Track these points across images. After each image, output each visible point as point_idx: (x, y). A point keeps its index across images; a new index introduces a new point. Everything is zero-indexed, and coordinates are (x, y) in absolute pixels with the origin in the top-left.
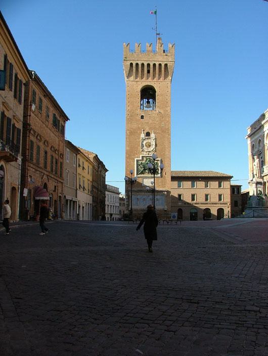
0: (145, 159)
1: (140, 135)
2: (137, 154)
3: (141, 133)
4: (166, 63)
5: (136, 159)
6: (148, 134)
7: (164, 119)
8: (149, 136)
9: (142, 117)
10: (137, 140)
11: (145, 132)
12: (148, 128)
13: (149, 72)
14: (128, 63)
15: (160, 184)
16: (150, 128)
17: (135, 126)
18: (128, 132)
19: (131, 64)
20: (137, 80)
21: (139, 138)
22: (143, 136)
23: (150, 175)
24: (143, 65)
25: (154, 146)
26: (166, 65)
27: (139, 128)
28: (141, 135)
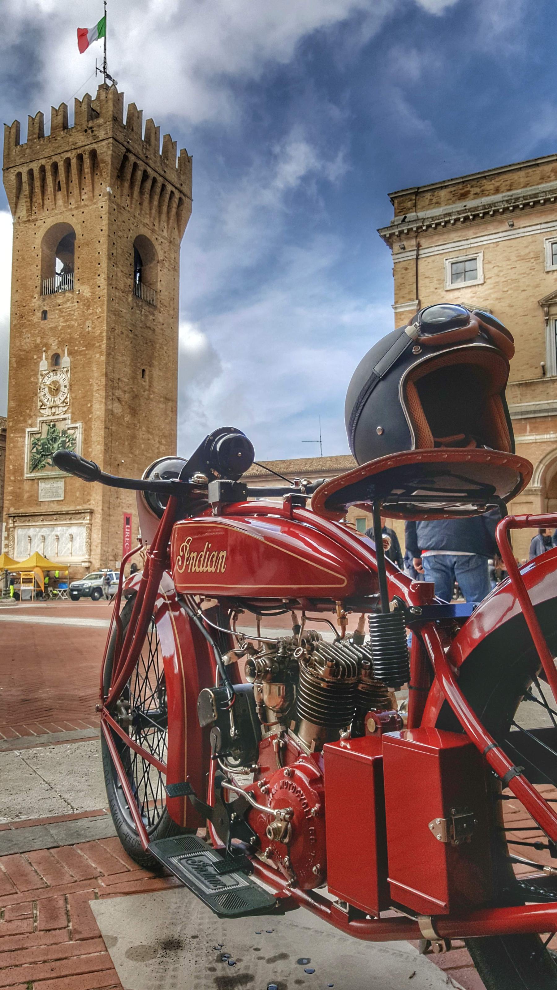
0: (45, 428)
1: (37, 364)
2: (30, 417)
3: (41, 358)
5: (28, 430)
6: (56, 359)
10: (32, 379)
11: (50, 353)
16: (61, 344)
17: (28, 341)
18: (14, 360)
21: (36, 375)
22: (44, 365)
24: (42, 169)
26: (93, 154)
27: (37, 346)
28: (41, 364)
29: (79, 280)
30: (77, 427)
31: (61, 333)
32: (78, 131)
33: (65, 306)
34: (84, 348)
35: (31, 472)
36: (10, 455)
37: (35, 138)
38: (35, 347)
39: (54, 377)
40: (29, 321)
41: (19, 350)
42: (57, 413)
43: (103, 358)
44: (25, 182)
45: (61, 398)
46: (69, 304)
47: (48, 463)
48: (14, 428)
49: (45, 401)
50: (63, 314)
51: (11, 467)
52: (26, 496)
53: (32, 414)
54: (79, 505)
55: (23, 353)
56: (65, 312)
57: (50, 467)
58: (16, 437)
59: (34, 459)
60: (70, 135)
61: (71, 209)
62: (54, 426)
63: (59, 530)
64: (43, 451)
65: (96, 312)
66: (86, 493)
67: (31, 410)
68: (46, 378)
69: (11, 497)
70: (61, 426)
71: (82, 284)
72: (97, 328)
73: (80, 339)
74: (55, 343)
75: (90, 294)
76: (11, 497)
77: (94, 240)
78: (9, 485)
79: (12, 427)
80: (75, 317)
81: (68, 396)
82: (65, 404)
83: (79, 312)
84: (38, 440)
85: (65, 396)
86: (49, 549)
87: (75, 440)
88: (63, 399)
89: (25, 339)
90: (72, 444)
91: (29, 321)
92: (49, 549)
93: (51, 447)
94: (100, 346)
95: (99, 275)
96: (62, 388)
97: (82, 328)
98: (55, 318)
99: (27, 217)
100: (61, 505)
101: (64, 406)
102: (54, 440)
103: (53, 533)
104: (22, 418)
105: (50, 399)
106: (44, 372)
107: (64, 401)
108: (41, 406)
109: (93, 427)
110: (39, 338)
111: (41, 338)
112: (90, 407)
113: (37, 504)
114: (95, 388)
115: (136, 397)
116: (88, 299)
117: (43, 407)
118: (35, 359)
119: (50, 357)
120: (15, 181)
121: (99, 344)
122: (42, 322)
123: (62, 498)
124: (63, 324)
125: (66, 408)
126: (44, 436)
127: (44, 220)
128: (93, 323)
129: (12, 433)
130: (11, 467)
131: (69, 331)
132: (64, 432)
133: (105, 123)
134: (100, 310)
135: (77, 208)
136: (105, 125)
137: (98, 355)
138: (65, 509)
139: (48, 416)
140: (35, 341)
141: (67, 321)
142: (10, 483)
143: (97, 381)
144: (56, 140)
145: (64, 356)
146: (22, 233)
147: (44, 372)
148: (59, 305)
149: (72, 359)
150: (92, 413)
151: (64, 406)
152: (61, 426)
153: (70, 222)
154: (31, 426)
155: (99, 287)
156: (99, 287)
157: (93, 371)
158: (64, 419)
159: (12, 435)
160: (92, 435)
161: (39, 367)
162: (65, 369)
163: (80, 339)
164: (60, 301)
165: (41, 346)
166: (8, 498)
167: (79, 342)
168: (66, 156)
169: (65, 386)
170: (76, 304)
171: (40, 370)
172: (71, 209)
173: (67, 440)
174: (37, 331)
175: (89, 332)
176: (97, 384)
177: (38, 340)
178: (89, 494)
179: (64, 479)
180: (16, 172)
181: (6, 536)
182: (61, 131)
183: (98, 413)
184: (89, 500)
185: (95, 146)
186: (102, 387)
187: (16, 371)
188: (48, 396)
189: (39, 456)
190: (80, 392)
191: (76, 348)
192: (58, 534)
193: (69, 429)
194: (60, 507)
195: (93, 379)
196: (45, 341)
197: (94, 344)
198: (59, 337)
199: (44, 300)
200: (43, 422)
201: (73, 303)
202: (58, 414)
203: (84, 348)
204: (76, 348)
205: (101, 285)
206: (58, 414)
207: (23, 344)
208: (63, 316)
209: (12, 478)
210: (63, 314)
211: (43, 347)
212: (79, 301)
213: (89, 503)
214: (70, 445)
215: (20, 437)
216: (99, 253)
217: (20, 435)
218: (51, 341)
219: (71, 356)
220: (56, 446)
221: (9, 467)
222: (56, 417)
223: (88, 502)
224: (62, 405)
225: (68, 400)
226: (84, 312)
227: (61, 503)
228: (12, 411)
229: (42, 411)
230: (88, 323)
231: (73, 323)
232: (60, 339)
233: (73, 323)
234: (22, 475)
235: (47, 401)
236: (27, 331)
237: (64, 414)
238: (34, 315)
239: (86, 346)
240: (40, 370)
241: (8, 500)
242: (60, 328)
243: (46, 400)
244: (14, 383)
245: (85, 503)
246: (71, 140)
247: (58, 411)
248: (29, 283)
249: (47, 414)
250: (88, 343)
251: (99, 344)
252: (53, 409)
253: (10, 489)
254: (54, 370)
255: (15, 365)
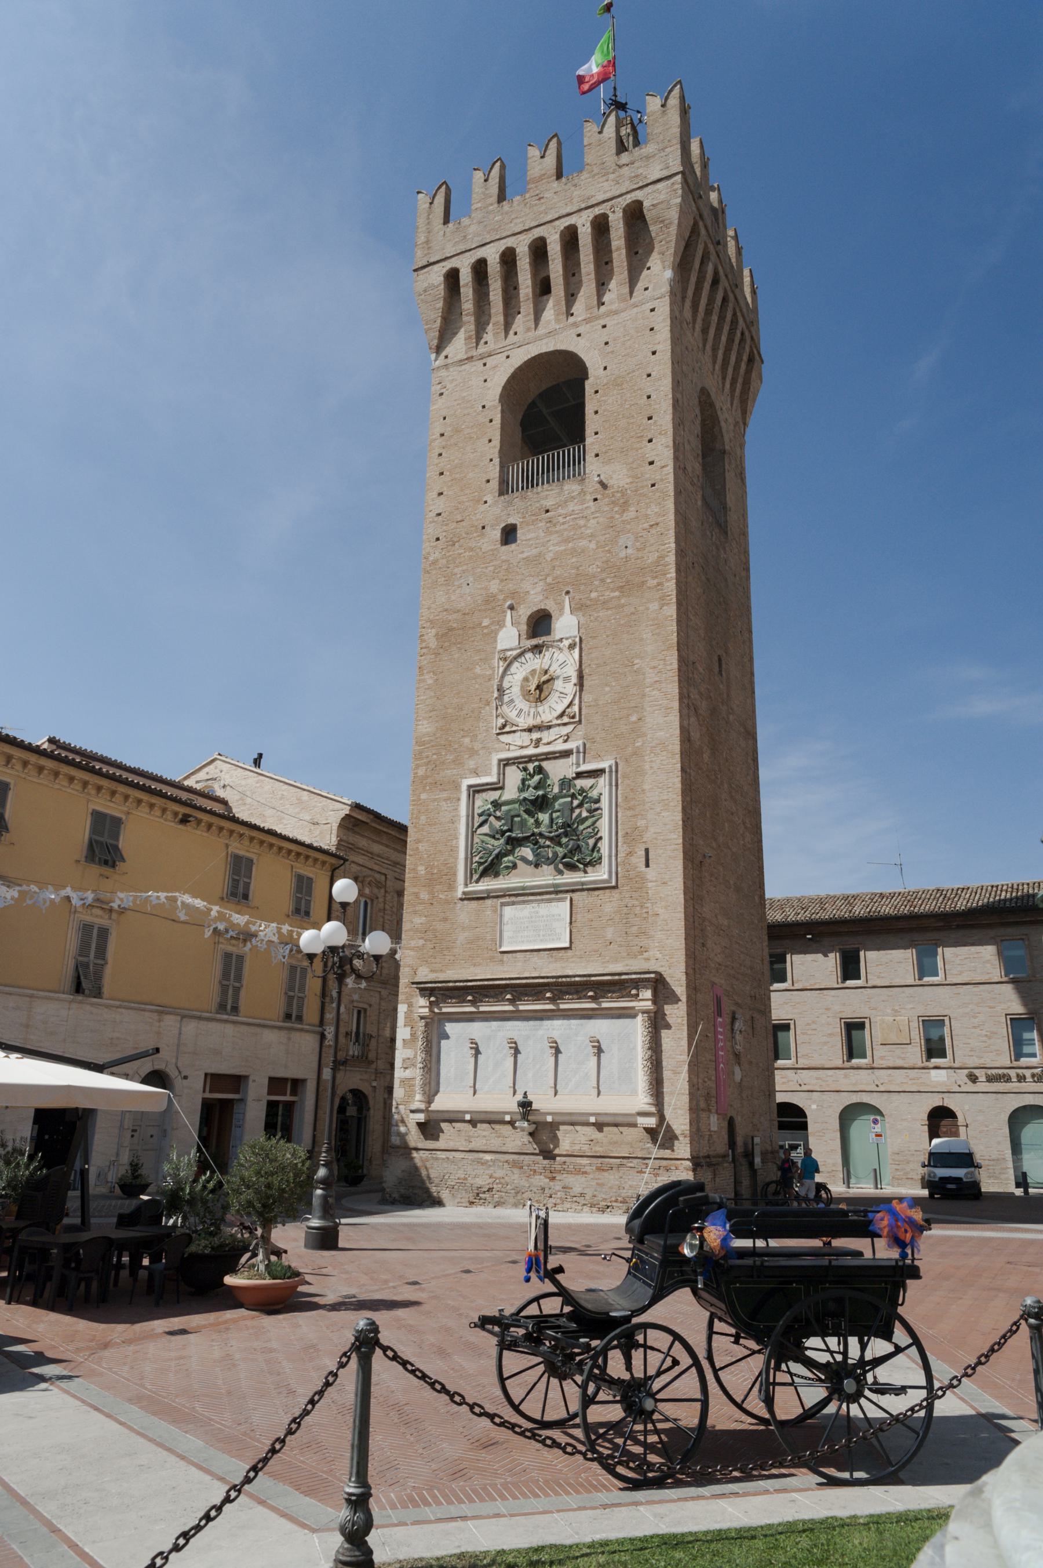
0: (514, 776)
2: (473, 752)
3: (501, 624)
4: (629, 198)
7: (631, 514)
8: (548, 632)
9: (509, 534)
10: (478, 670)
11: (525, 612)
12: (541, 585)
13: (543, 288)
14: (436, 276)
15: (610, 933)
19: (452, 277)
20: (482, 349)
23: (546, 876)
25: (570, 688)
27: (490, 600)
28: (502, 635)
29: (597, 455)
30: (602, 771)
31: (554, 567)
32: (594, 175)
33: (561, 511)
34: (617, 594)
35: (477, 882)
36: (418, 841)
37: (492, 205)
38: (487, 602)
39: (533, 662)
40: (471, 549)
41: (446, 610)
42: (544, 741)
43: (671, 611)
44: (466, 285)
45: (553, 706)
46: (571, 506)
47: (524, 859)
48: (429, 780)
49: (512, 715)
50: (558, 528)
51: (422, 870)
52: (462, 937)
53: (477, 746)
54: (616, 961)
55: (455, 616)
56: (563, 524)
57: (531, 869)
58: (435, 800)
59: (484, 849)
60: (575, 186)
61: (575, 325)
62: (540, 770)
63: (556, 1028)
64: (510, 830)
65: (647, 515)
66: (634, 929)
67: (474, 739)
68: (516, 664)
69: (421, 942)
70: (558, 770)
71: (609, 461)
72: (647, 549)
73: (604, 575)
74: (539, 589)
75: (628, 480)
76: (421, 942)
77: (637, 373)
78: (415, 912)
79: (426, 777)
80: (589, 531)
81: (577, 701)
82: (566, 720)
83: (601, 520)
84: (496, 804)
85: (567, 702)
86: (530, 1075)
87: (598, 801)
88: (560, 709)
89: (460, 587)
90: (589, 811)
91: (471, 549)
92: (530, 1075)
93: (532, 821)
94: (659, 584)
95: (650, 441)
96: (558, 685)
97: (609, 551)
98: (537, 538)
99: (466, 353)
100: (561, 959)
101: (565, 724)
102: (541, 803)
103: (541, 1032)
104: (450, 757)
105: (526, 709)
106: (509, 653)
107: (564, 712)
108: (504, 726)
109: (647, 767)
110: (497, 581)
111: (502, 581)
112: (635, 723)
113: (492, 959)
114: (651, 677)
115: (714, 711)
116: (623, 492)
117: (507, 729)
118: (486, 627)
119: (524, 619)
120: (442, 286)
121: (655, 582)
122: (505, 548)
123: (567, 945)
124: (557, 548)
125: (570, 728)
126: (511, 792)
127: (506, 354)
128: (636, 539)
129: (424, 790)
130: (422, 870)
131: (574, 560)
132: (566, 783)
133: (663, 150)
134: (656, 510)
135: (588, 321)
136: (663, 154)
137: (654, 606)
138: (576, 968)
139: (522, 747)
140: (486, 588)
141: (567, 541)
142: (420, 908)
143: (655, 663)
144: (539, 199)
145: (561, 614)
146: (455, 383)
147: (509, 653)
148: (547, 511)
149: (583, 620)
150: (644, 735)
151: (565, 724)
152: (558, 770)
153: (571, 349)
154: (476, 773)
155: (651, 463)
156: (651, 463)
157: (642, 640)
158: (566, 754)
159: (424, 796)
160: (646, 787)
161: (496, 641)
162: (566, 643)
163: (604, 575)
164: (548, 503)
165: (501, 597)
166: (413, 943)
167: (603, 580)
168: (567, 224)
169: (567, 679)
170: (592, 503)
171: (500, 646)
172: (575, 325)
173: (576, 803)
174: (493, 568)
175: (627, 558)
176: (654, 667)
177: (494, 587)
178: (643, 933)
179: (568, 896)
180: (444, 271)
181: (408, 1036)
182: (553, 181)
183: (661, 734)
184: (643, 950)
185: (638, 195)
186: (670, 674)
187: (437, 654)
188: (521, 704)
189: (496, 843)
190: (607, 689)
191: (594, 595)
192: (556, 1035)
193: (579, 775)
194: (558, 965)
195: (642, 658)
196: (511, 586)
197: (643, 583)
198: (548, 575)
199: (510, 503)
200: (506, 763)
201: (583, 502)
202: (549, 743)
203: (617, 594)
204: (594, 595)
205: (656, 459)
206: (549, 743)
207: (453, 598)
208: (557, 532)
209: (424, 895)
210: (558, 528)
211: (505, 600)
212: (599, 497)
213: (646, 955)
214: (585, 814)
215: (445, 800)
216: (649, 397)
217: (444, 795)
218: (526, 585)
219: (580, 614)
220: (544, 817)
221: (414, 870)
222: (543, 749)
223: (641, 953)
224: (559, 722)
225: (576, 708)
226: (612, 517)
227: (562, 953)
228: (423, 743)
229: (504, 738)
230: (622, 541)
231: (583, 543)
232: (549, 580)
233: (583, 543)
234: (451, 886)
235: (518, 715)
236: (464, 571)
237: (566, 741)
238: (482, 535)
239: (621, 588)
240: (500, 646)
241: (412, 949)
242: (549, 556)
243: (515, 712)
244: (430, 682)
245: (631, 955)
246: (576, 193)
247: (546, 736)
248: (471, 475)
249: (520, 743)
250: (627, 582)
251: (655, 582)
252: (535, 735)
253: (418, 920)
254: (536, 647)
255: (433, 644)
